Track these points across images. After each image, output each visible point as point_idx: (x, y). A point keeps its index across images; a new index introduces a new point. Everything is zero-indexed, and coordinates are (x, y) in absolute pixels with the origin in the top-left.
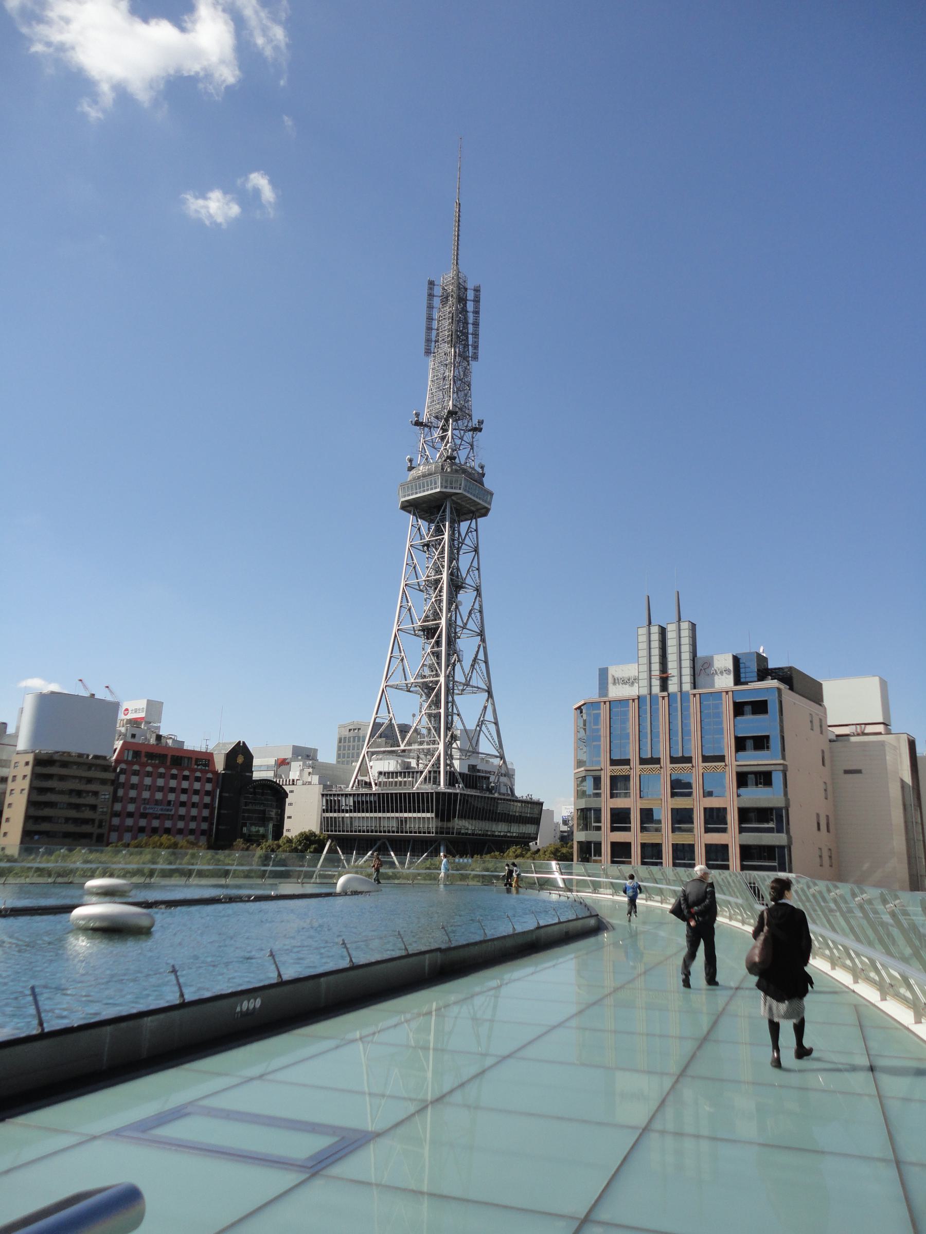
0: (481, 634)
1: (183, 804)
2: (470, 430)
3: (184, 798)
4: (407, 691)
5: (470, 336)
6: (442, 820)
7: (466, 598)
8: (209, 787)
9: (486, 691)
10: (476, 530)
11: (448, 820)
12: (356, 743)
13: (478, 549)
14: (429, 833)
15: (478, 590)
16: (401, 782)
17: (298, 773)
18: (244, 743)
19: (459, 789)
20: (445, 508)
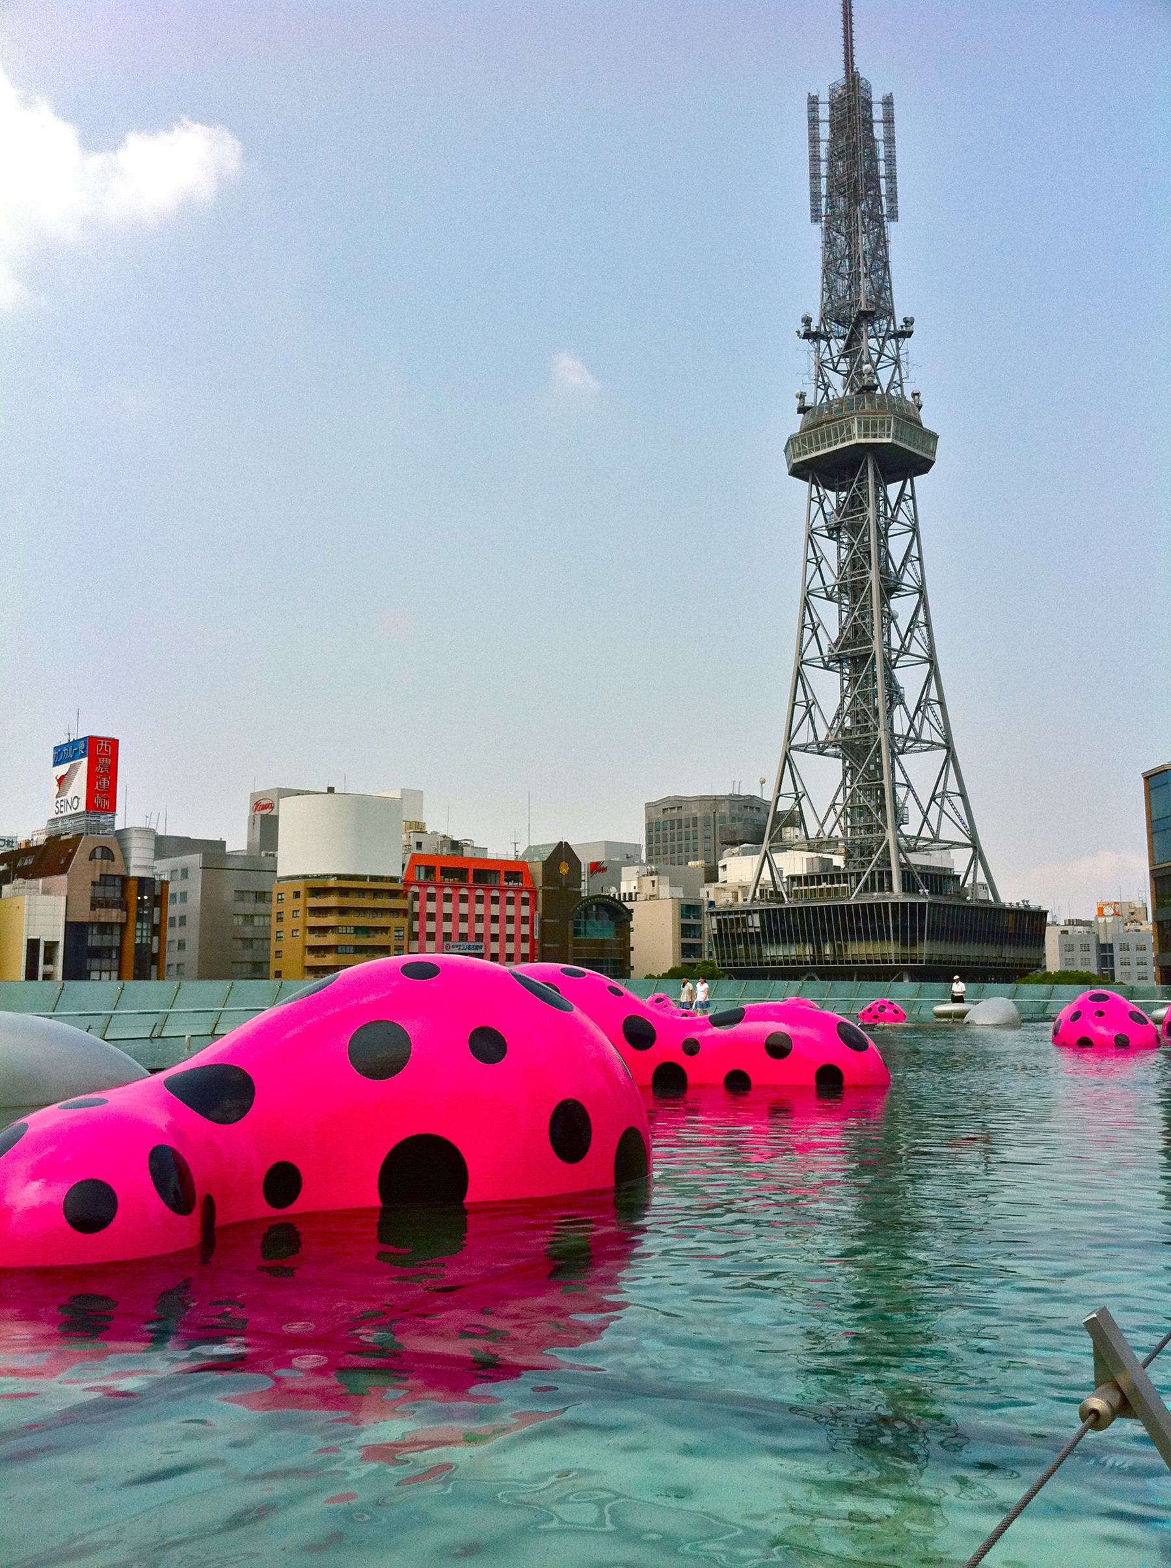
0: (931, 660)
1: (495, 938)
2: (891, 337)
3: (495, 928)
4: (820, 754)
5: (883, 181)
6: (904, 944)
7: (903, 606)
8: (525, 911)
9: (944, 747)
10: (913, 498)
11: (913, 944)
12: (676, 831)
13: (918, 528)
14: (885, 961)
15: (921, 591)
16: (829, 889)
17: (635, 883)
18: (566, 843)
19: (924, 896)
20: (866, 467)
